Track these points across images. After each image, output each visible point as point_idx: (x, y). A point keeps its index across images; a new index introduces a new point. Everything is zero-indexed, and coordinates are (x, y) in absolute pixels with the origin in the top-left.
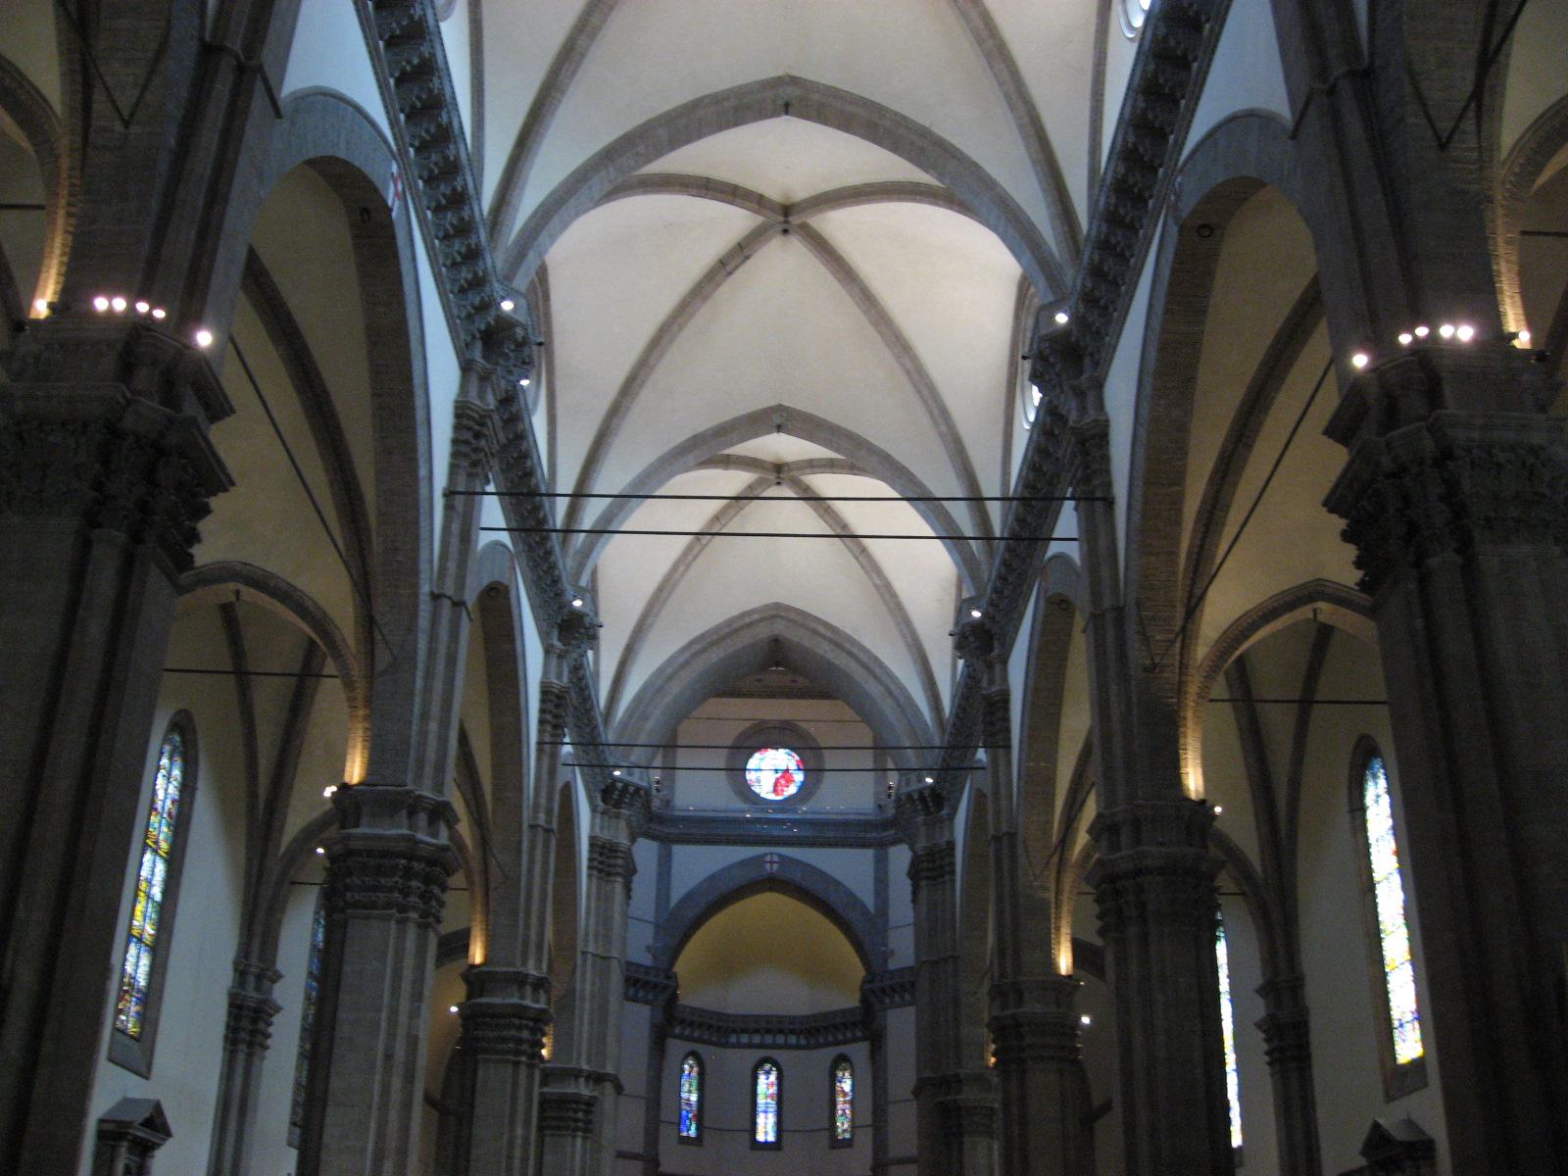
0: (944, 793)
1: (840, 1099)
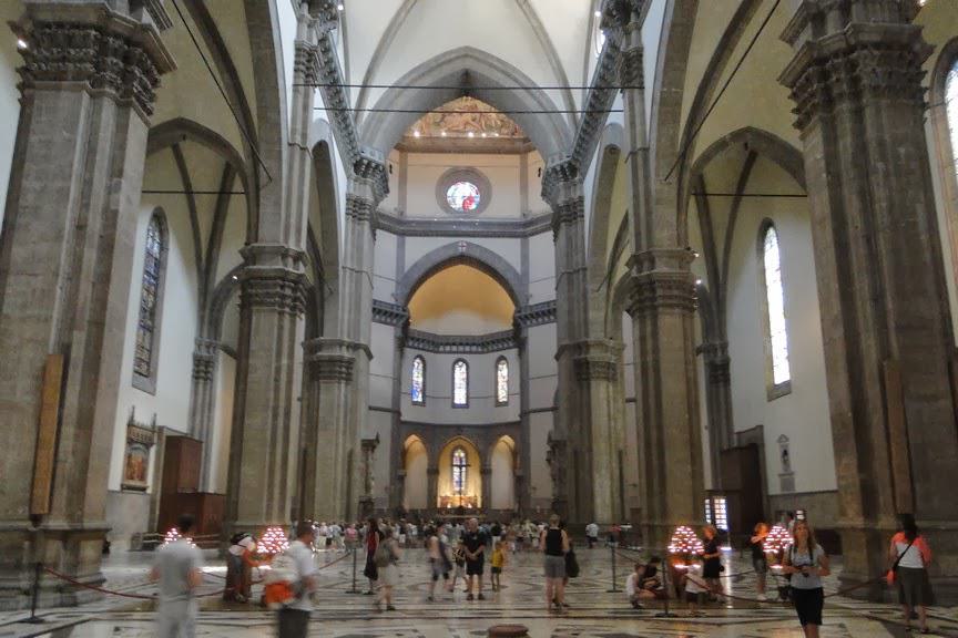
0: (578, 165)
1: (500, 380)
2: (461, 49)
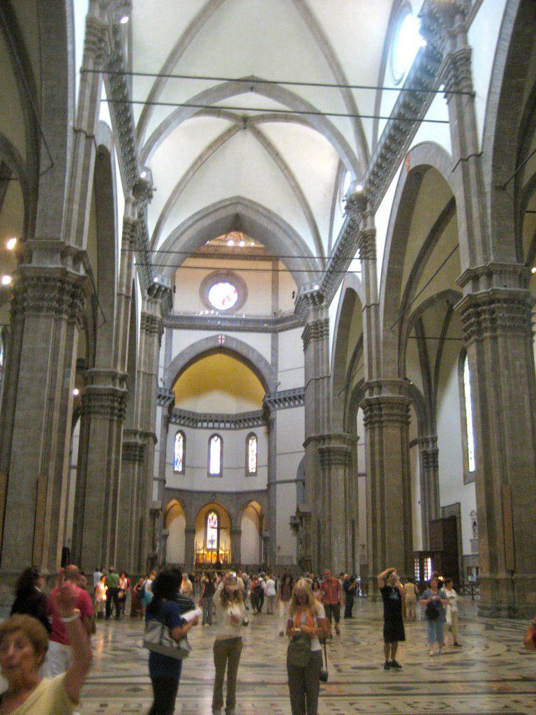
1: (250, 453)
2: (233, 198)
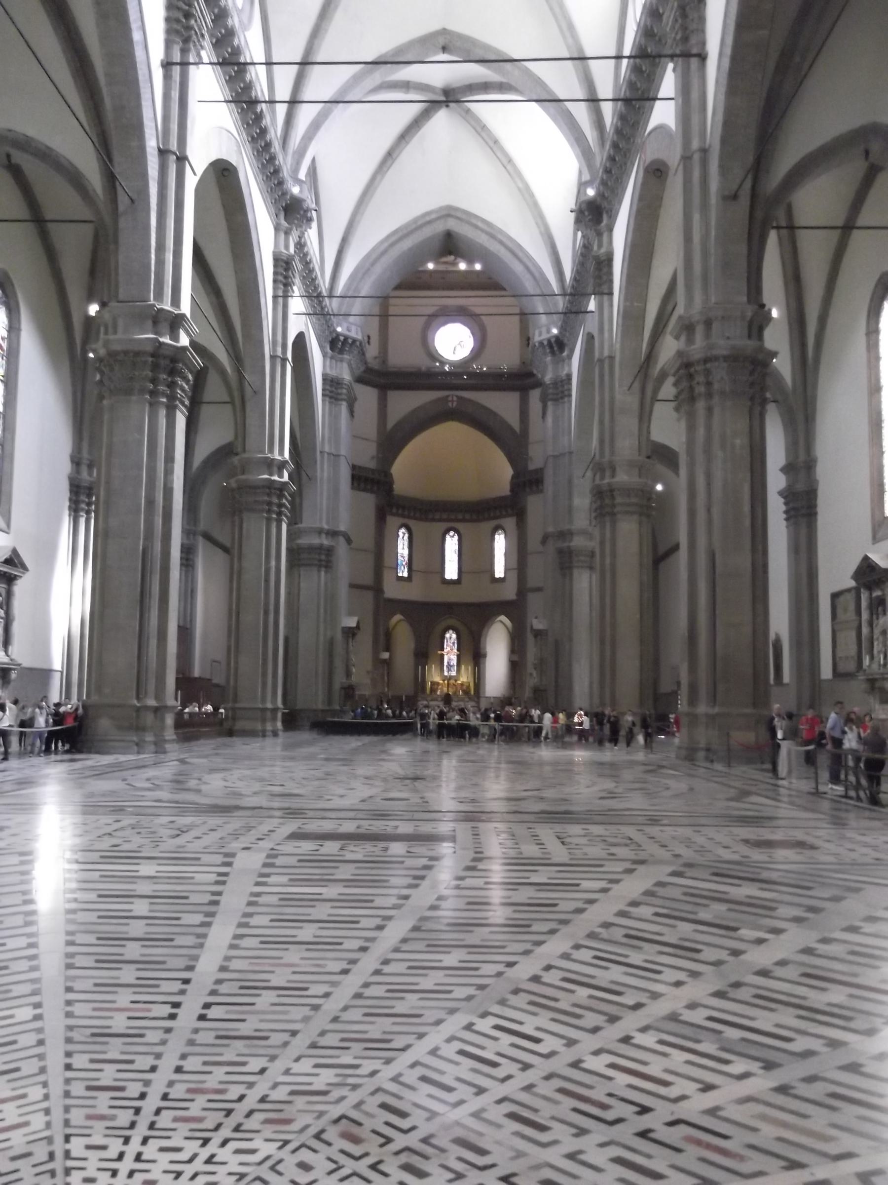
0: (566, 341)
2: (441, 209)
